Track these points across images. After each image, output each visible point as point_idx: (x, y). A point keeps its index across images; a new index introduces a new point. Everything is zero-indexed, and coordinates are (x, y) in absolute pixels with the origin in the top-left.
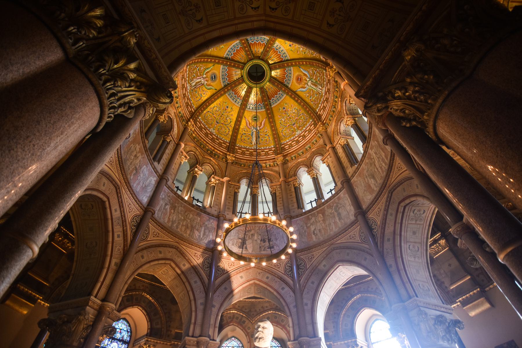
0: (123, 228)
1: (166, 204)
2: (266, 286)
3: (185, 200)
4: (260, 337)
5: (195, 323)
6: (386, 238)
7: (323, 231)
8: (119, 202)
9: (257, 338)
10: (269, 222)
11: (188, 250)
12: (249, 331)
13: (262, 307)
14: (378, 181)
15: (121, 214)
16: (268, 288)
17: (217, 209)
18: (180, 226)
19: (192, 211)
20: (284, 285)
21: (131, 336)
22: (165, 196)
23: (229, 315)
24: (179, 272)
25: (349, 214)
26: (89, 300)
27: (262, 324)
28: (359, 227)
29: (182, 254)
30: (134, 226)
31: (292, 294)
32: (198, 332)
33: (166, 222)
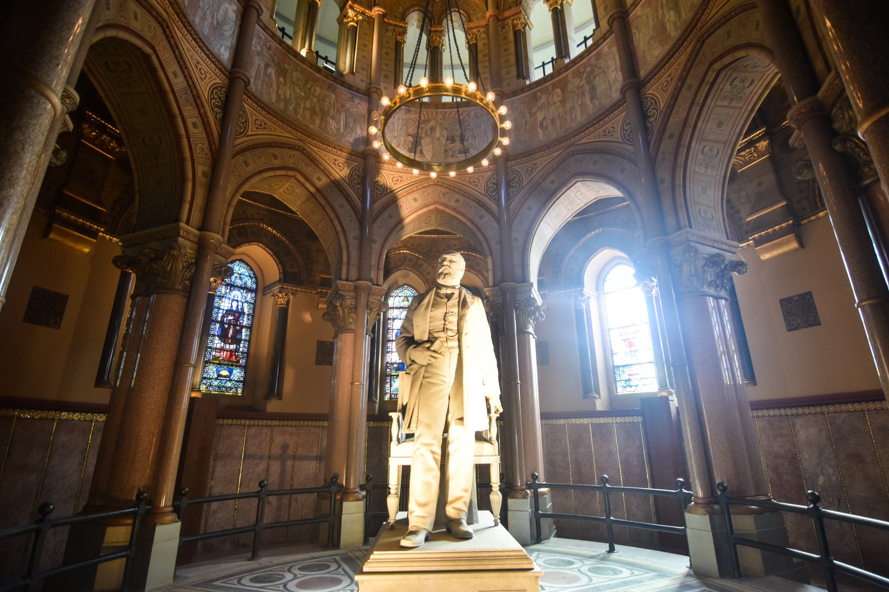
0: (199, 110)
1: (267, 66)
2: (454, 214)
3: (302, 57)
6: (667, 134)
7: (558, 122)
8: (176, 57)
9: (441, 273)
10: (463, 95)
11: (323, 153)
12: (428, 277)
14: (684, 16)
15: (188, 82)
16: (458, 216)
17: (364, 78)
18: (301, 110)
19: (318, 80)
20: (483, 212)
21: (257, 283)
22: (262, 48)
24: (312, 190)
25: (610, 89)
26: (179, 228)
27: (448, 257)
28: (623, 114)
29: (313, 161)
30: (218, 107)
32: (354, 274)
33: (274, 100)
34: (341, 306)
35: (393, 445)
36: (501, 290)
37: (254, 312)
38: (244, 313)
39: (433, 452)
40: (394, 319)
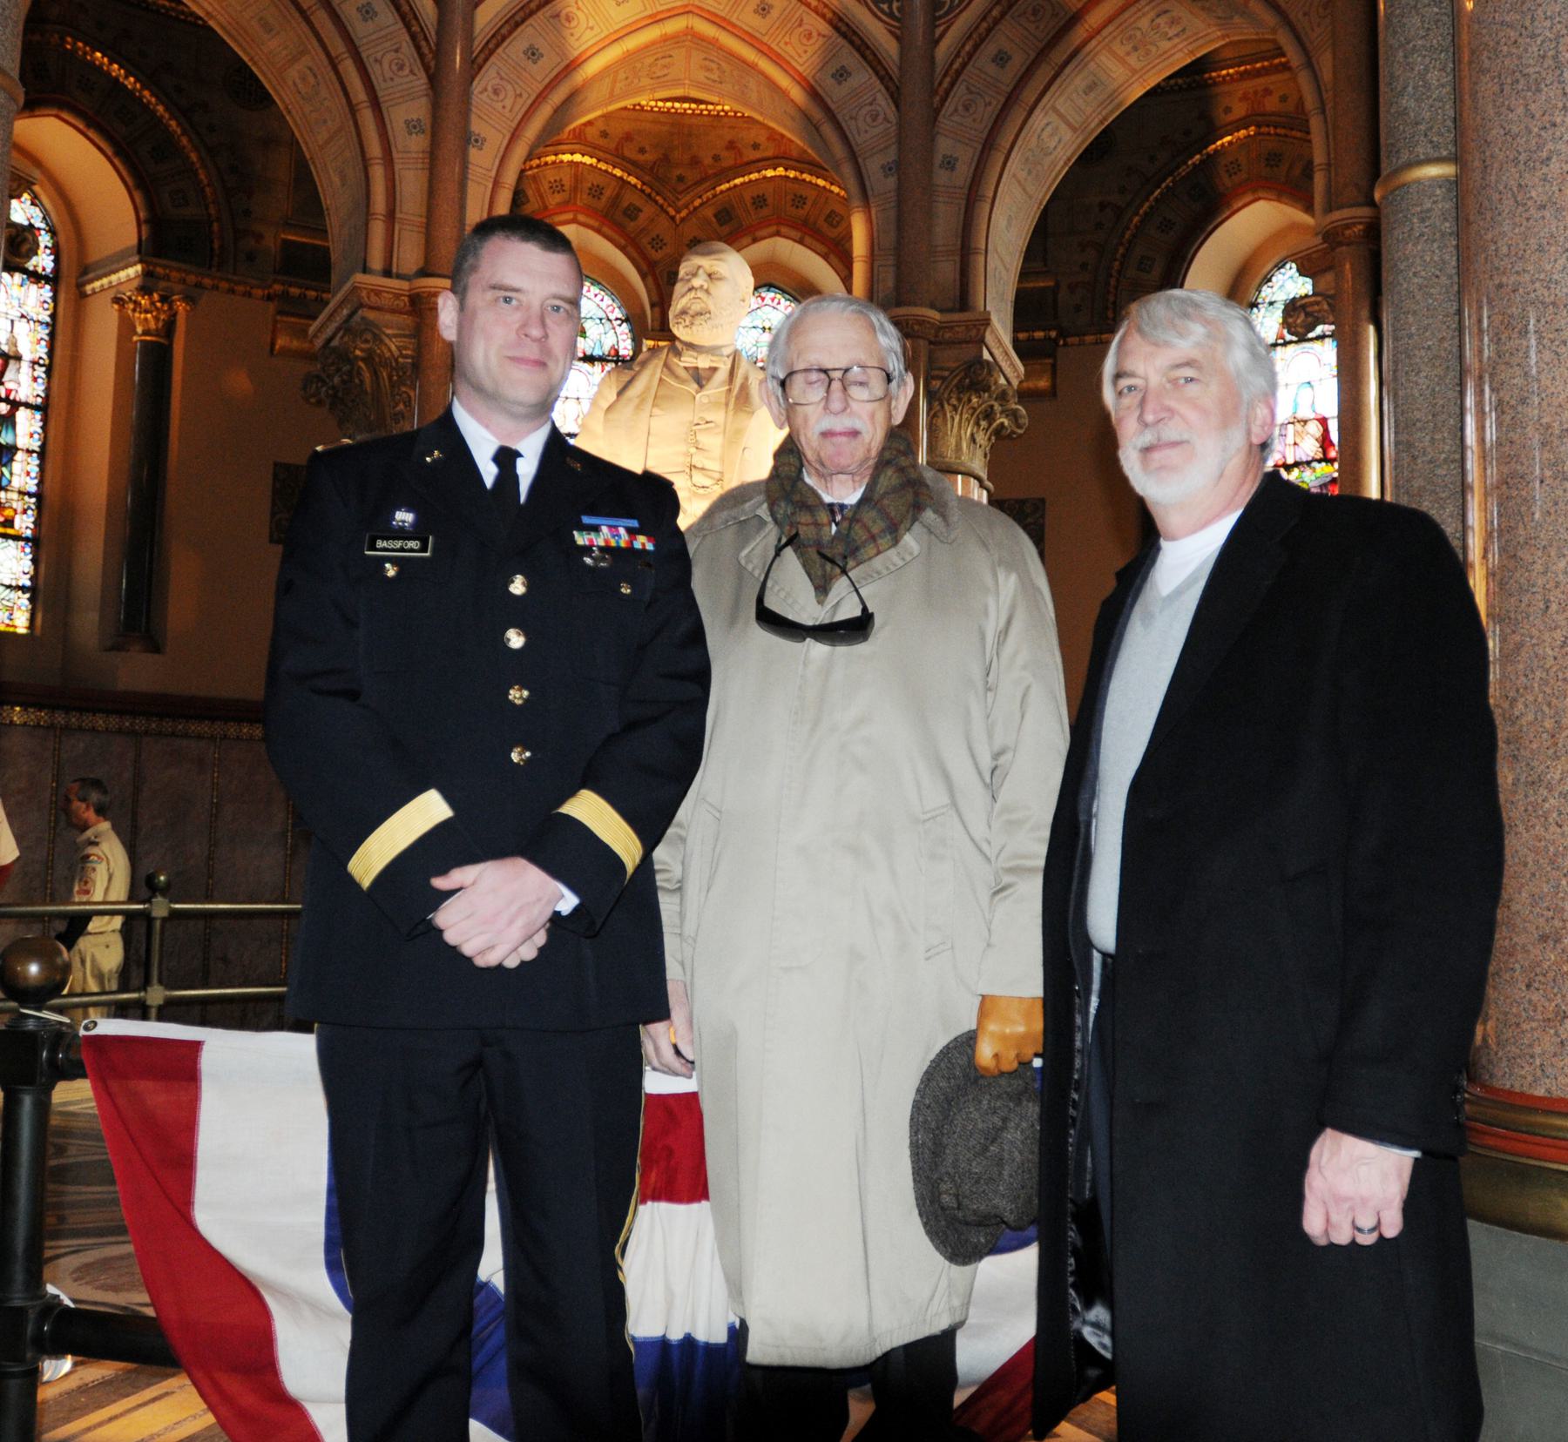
2: (749, 54)
4: (696, 307)
5: (391, 216)
13: (731, 145)
23: (551, 175)
31: (884, 103)
32: (409, 255)
37: (51, 354)
38: (18, 358)
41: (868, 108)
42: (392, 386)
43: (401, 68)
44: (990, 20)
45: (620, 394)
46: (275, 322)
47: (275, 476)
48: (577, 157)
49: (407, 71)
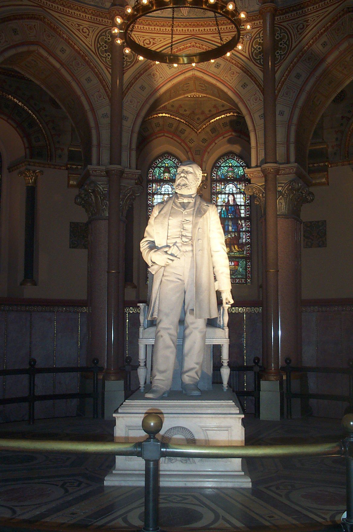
4: (183, 183)
5: (99, 145)
12: (191, 145)
34: (94, 191)
35: (141, 329)
36: (263, 171)
39: (170, 334)
40: (154, 194)
41: (253, 97)
42: (102, 200)
43: (100, 97)
44: (293, 63)
45: (159, 213)
46: (68, 177)
47: (71, 226)
48: (164, 115)
49: (102, 97)
